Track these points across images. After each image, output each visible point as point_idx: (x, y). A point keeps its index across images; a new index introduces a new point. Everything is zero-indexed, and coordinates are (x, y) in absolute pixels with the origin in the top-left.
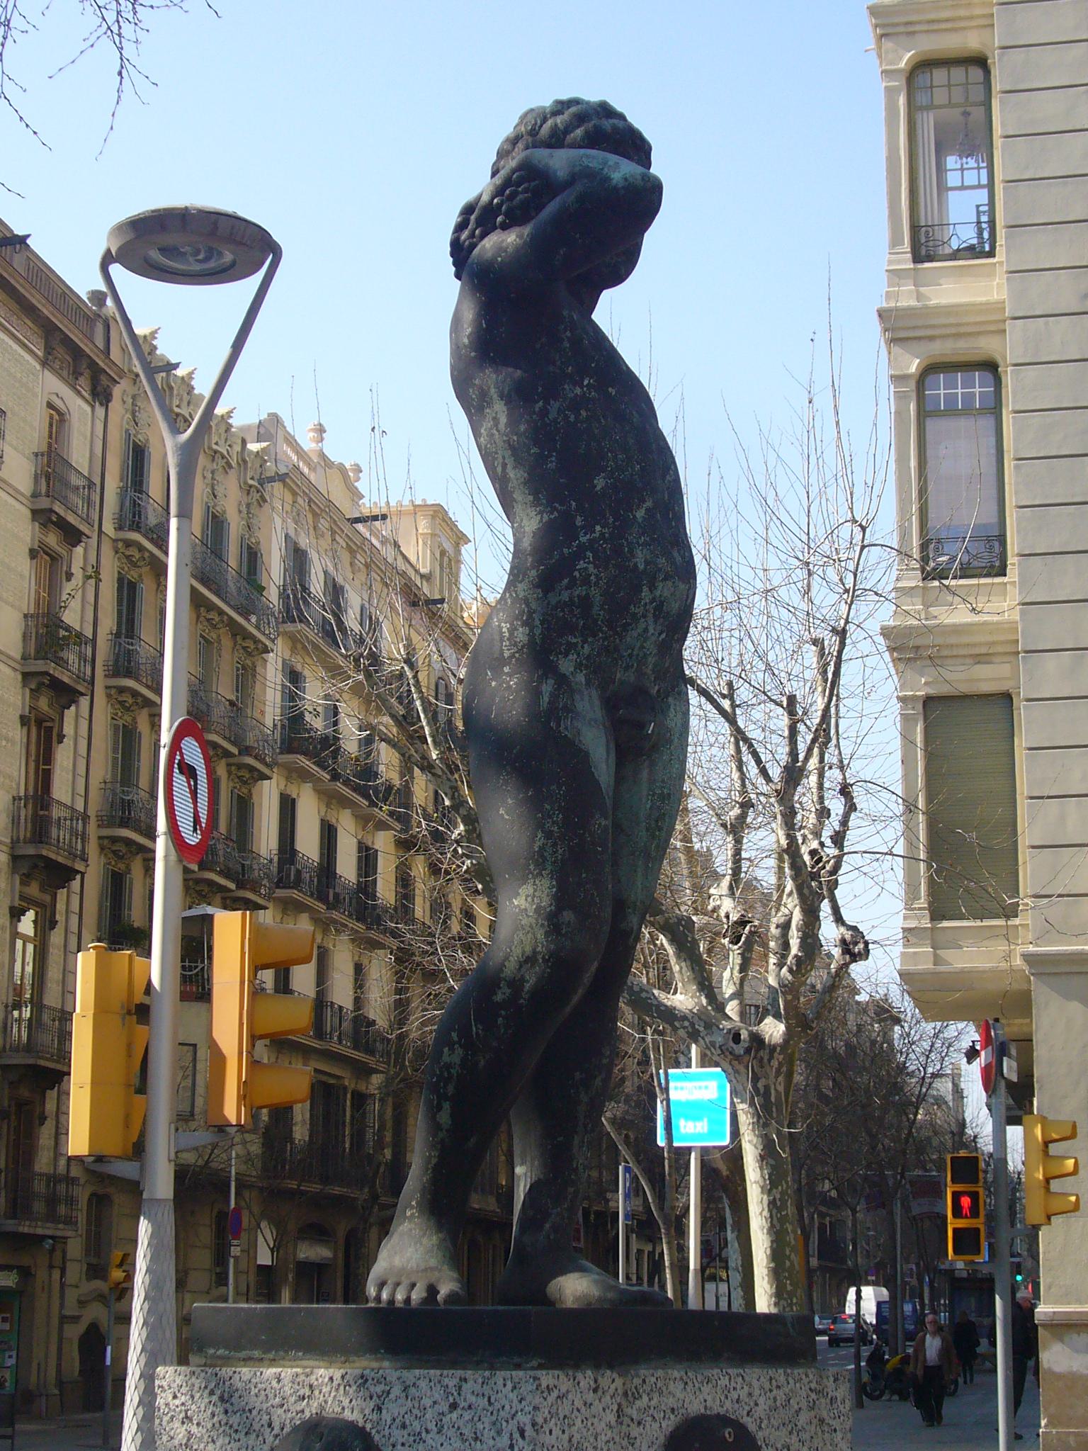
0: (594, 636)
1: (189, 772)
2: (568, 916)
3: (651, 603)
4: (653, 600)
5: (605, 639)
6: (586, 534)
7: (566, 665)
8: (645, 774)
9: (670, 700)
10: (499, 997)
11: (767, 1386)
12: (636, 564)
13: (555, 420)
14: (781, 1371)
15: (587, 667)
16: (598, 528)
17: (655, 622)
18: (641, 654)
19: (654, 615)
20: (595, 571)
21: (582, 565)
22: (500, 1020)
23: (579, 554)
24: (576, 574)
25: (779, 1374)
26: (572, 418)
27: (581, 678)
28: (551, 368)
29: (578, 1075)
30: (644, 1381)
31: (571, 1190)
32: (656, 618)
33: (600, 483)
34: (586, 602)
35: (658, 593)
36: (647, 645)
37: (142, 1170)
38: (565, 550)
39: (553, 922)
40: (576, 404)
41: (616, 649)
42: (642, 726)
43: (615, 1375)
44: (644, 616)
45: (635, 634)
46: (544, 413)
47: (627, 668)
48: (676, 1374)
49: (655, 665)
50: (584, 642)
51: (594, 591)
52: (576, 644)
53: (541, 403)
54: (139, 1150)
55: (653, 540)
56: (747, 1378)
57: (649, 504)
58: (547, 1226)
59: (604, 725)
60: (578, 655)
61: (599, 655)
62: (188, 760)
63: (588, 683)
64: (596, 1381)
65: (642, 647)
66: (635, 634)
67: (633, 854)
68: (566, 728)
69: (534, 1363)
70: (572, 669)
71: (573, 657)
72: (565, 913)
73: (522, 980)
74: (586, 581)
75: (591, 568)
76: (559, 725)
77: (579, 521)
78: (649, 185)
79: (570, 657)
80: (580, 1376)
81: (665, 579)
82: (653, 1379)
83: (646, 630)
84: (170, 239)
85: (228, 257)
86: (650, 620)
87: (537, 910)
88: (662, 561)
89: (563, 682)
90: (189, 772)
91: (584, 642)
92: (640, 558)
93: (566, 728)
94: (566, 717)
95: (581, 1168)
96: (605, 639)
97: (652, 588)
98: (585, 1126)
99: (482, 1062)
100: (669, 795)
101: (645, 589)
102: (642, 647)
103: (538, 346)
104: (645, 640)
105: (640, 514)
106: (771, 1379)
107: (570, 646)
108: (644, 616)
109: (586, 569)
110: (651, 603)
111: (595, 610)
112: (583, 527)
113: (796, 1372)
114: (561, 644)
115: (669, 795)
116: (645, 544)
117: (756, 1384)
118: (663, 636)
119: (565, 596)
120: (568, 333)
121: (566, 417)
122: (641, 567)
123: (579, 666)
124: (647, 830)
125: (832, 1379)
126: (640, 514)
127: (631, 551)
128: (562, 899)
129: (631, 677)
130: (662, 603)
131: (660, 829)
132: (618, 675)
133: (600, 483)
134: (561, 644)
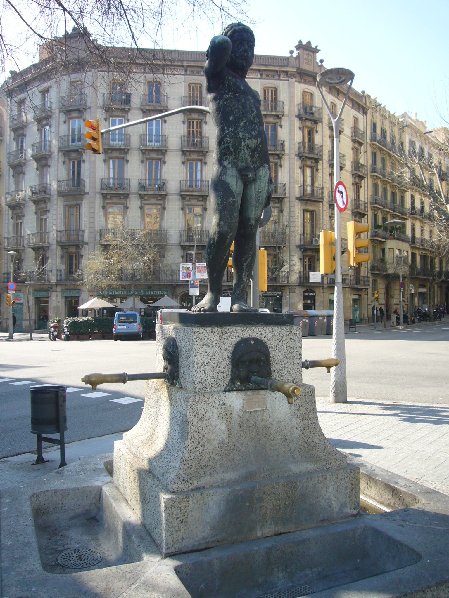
1: (341, 193)
2: (222, 223)
7: (225, 163)
8: (253, 187)
10: (211, 242)
21: (226, 138)
23: (225, 136)
25: (276, 328)
27: (230, 166)
33: (231, 118)
34: (228, 148)
35: (247, 143)
37: (335, 276)
39: (219, 225)
40: (226, 100)
42: (248, 176)
46: (219, 103)
47: (242, 162)
49: (251, 161)
54: (334, 272)
57: (244, 121)
59: (236, 177)
62: (340, 190)
63: (232, 167)
71: (227, 161)
74: (227, 142)
75: (228, 139)
77: (226, 128)
80: (207, 329)
83: (245, 152)
84: (329, 76)
85: (344, 78)
86: (245, 149)
88: (247, 135)
90: (341, 193)
92: (241, 135)
97: (245, 142)
105: (242, 124)
107: (226, 159)
116: (242, 131)
117: (267, 330)
119: (223, 147)
122: (241, 137)
123: (229, 163)
126: (242, 124)
128: (221, 219)
129: (244, 164)
133: (231, 118)
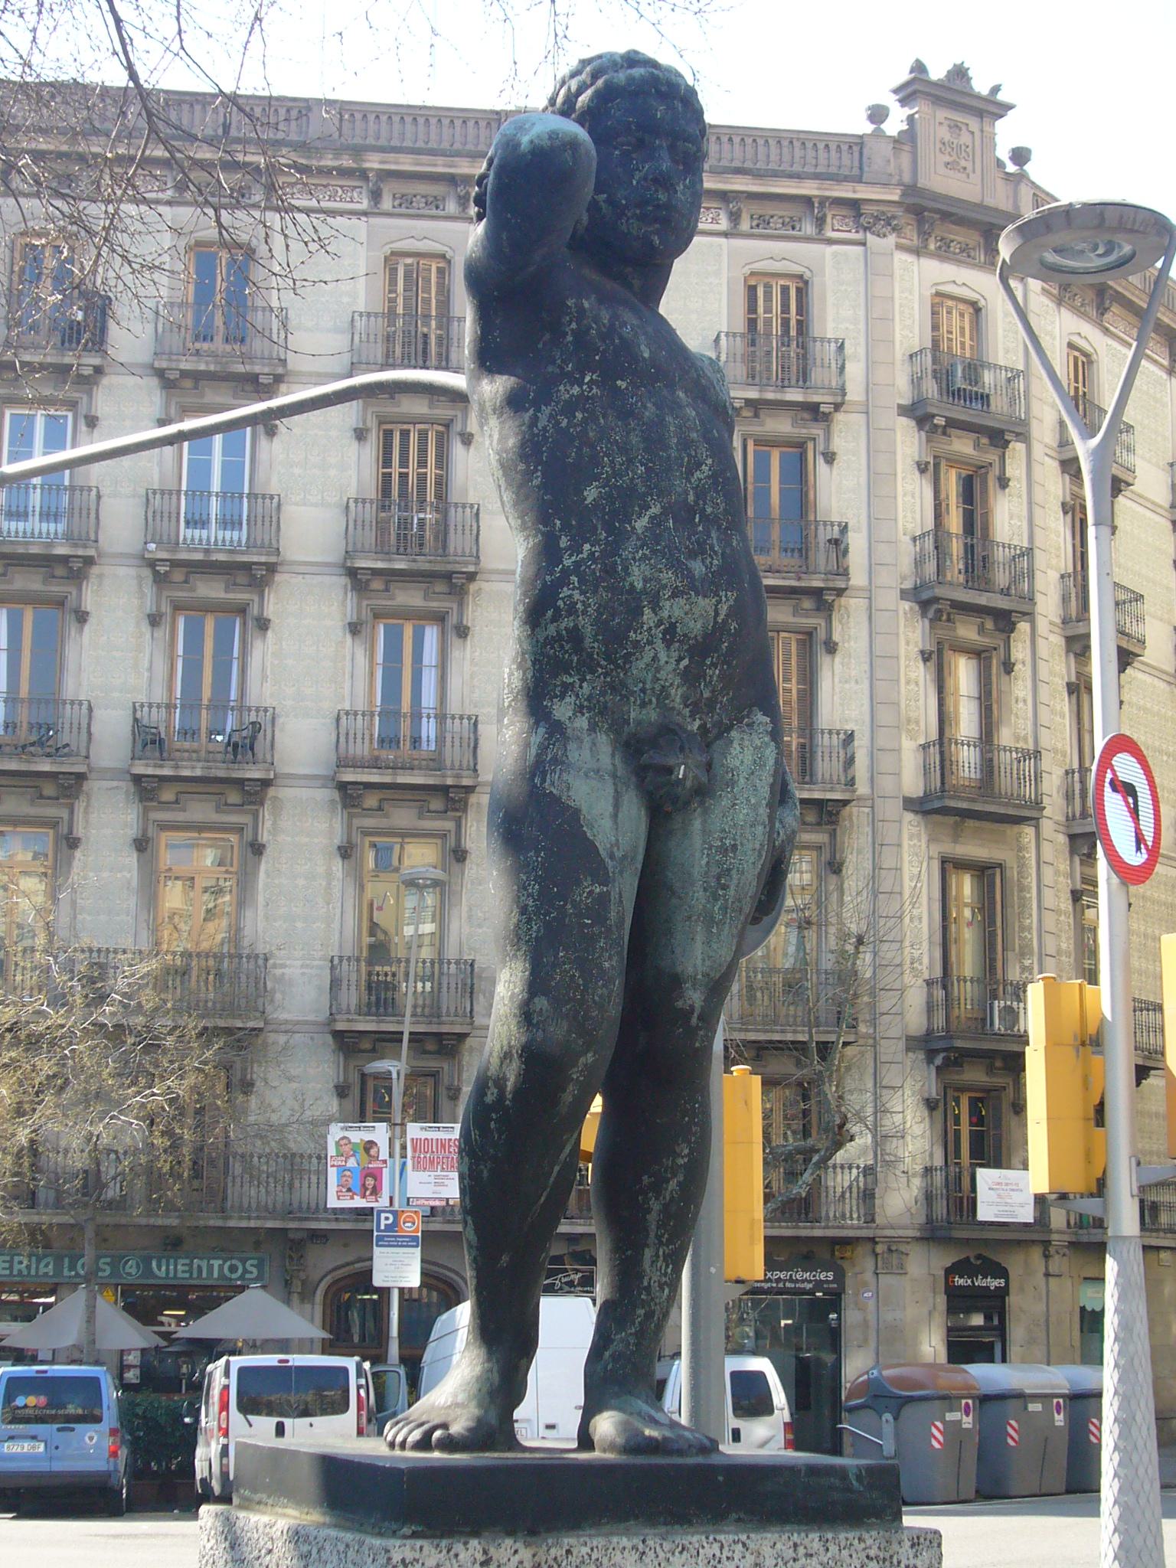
0: (593, 672)
1: (1127, 790)
2: (541, 1003)
3: (657, 626)
4: (660, 623)
5: (606, 675)
6: (571, 555)
7: (562, 710)
8: (697, 824)
9: (734, 734)
10: (489, 1098)
11: (791, 1553)
12: (632, 585)
13: (544, 429)
14: (814, 1536)
15: (589, 709)
16: (587, 547)
17: (668, 647)
18: (657, 687)
19: (664, 639)
20: (582, 598)
21: (565, 592)
22: (492, 1125)
23: (563, 581)
24: (560, 603)
25: (813, 1540)
26: (564, 423)
27: (582, 722)
28: (550, 369)
29: (646, 1179)
30: (568, 1552)
31: (641, 1312)
32: (668, 644)
33: (591, 494)
34: (575, 636)
35: (665, 614)
36: (662, 675)
37: (1105, 1208)
38: (548, 578)
39: (527, 1015)
40: (569, 409)
41: (623, 684)
42: (669, 770)
43: (519, 1545)
44: (650, 643)
45: (641, 664)
46: (534, 420)
47: (644, 705)
48: (625, 1541)
49: (685, 699)
50: (582, 680)
51: (582, 621)
52: (572, 684)
53: (531, 411)
54: (1101, 1187)
55: (654, 552)
56: (751, 1545)
57: (655, 510)
58: (607, 1354)
59: (614, 776)
60: (577, 696)
61: (603, 693)
62: (1122, 777)
63: (593, 728)
64: (485, 1552)
65: (656, 680)
66: (641, 664)
67: (689, 918)
68: (553, 784)
69: (406, 1531)
70: (570, 714)
71: (570, 699)
72: (536, 1000)
73: (505, 1079)
74: (572, 610)
75: (577, 595)
76: (544, 781)
77: (564, 542)
78: (558, 143)
79: (567, 699)
80: (458, 1547)
81: (674, 596)
82: (585, 1550)
83: (655, 659)
84: (1059, 238)
85: (1127, 249)
86: (659, 645)
87: (511, 997)
88: (667, 577)
89: (557, 731)
90: (1127, 790)
91: (582, 680)
92: (637, 577)
93: (553, 784)
94: (554, 771)
95: (655, 1286)
96: (606, 675)
97: (656, 607)
98: (659, 1237)
99: (485, 1174)
100: (734, 847)
101: (646, 611)
102: (656, 680)
103: (540, 346)
104: (658, 670)
105: (641, 524)
106: (795, 1545)
107: (567, 688)
108: (650, 643)
109: (570, 596)
110: (657, 626)
111: (588, 642)
112: (566, 549)
113: (842, 1536)
114: (556, 686)
115: (734, 847)
116: (644, 558)
117: (767, 1551)
118: (685, 662)
119: (552, 630)
120: (574, 326)
121: (558, 423)
122: (639, 585)
123: (580, 709)
124: (705, 890)
125: (907, 1544)
126: (641, 524)
127: (626, 569)
128: (536, 985)
129: (652, 715)
130: (673, 626)
131: (725, 887)
132: (633, 715)
133: (591, 494)
134: (556, 686)
